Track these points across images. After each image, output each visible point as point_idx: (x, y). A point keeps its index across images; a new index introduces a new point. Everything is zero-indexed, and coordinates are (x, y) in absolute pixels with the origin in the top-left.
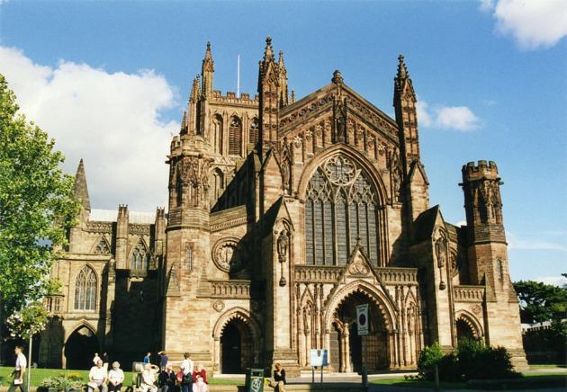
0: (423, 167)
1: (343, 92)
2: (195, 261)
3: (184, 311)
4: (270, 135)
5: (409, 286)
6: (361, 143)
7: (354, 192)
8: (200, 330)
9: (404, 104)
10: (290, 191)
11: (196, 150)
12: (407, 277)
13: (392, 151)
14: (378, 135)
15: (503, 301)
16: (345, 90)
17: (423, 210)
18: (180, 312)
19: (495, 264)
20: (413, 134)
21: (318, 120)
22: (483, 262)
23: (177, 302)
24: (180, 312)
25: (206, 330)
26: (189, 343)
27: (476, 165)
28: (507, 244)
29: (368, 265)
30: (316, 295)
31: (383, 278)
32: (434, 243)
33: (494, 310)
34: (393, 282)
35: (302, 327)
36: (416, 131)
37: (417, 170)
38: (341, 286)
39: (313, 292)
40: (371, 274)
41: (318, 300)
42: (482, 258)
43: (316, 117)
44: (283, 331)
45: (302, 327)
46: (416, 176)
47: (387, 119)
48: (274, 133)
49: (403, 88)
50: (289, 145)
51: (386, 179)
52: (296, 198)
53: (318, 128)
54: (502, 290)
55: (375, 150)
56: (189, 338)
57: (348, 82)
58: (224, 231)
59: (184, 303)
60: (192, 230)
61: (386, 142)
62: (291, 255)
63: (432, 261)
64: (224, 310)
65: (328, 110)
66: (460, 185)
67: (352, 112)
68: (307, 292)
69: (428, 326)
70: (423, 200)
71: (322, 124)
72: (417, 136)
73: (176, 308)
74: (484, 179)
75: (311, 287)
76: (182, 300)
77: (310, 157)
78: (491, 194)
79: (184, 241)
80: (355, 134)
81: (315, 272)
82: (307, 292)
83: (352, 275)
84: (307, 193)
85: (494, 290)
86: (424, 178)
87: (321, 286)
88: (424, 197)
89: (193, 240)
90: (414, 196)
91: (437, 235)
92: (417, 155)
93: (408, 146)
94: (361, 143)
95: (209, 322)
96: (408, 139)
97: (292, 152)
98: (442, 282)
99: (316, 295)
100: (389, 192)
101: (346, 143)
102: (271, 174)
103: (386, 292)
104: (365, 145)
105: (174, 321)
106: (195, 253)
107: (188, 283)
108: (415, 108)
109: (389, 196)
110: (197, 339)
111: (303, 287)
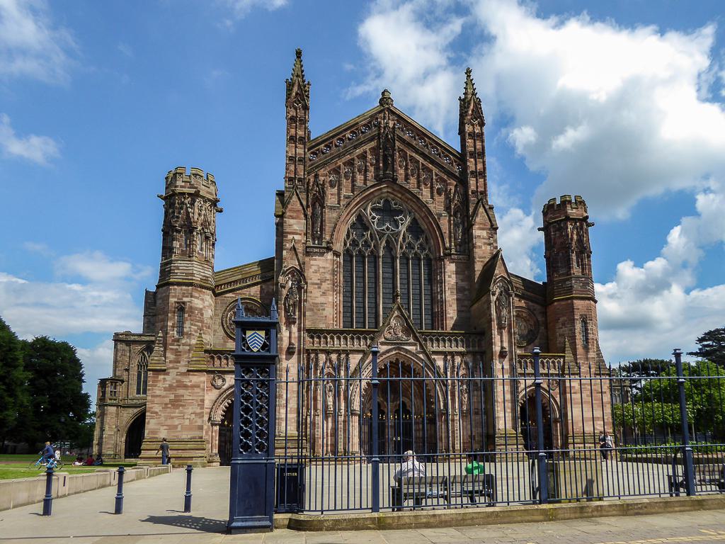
0: (491, 208)
2: (187, 325)
3: (171, 388)
4: (296, 169)
6: (413, 180)
7: (404, 241)
8: (191, 411)
9: (468, 128)
10: (320, 238)
14: (435, 170)
16: (393, 113)
18: (165, 389)
19: (578, 326)
20: (480, 166)
21: (359, 151)
23: (161, 377)
24: (165, 389)
25: (198, 411)
26: (176, 427)
27: (558, 202)
28: (596, 302)
29: (408, 330)
30: (339, 366)
31: (429, 344)
32: (494, 298)
34: (441, 349)
35: (320, 406)
36: (484, 163)
37: (481, 210)
40: (412, 340)
41: (342, 373)
43: (355, 147)
45: (320, 406)
46: (481, 218)
47: (446, 150)
49: (469, 107)
51: (444, 223)
52: (329, 249)
53: (358, 163)
55: (432, 188)
56: (176, 422)
59: (170, 378)
60: (184, 287)
61: (445, 177)
62: (302, 315)
63: (490, 321)
64: (225, 387)
65: (371, 139)
66: (539, 229)
70: (488, 247)
71: (363, 156)
72: (484, 168)
73: (160, 384)
74: (568, 218)
76: (168, 374)
77: (348, 197)
78: (575, 237)
79: (172, 300)
80: (406, 169)
81: (339, 338)
82: (328, 364)
84: (345, 244)
85: (576, 359)
86: (490, 220)
87: (347, 355)
88: (490, 244)
89: (185, 299)
90: (478, 242)
91: (496, 289)
92: (484, 193)
93: (472, 182)
95: (203, 401)
96: (472, 172)
97: (324, 192)
98: (502, 348)
100: (447, 240)
101: (395, 180)
102: (293, 218)
103: (432, 362)
104: (419, 182)
105: (156, 400)
106: (186, 315)
107: (177, 353)
108: (482, 134)
109: (448, 245)
110: (187, 422)
111: (322, 357)
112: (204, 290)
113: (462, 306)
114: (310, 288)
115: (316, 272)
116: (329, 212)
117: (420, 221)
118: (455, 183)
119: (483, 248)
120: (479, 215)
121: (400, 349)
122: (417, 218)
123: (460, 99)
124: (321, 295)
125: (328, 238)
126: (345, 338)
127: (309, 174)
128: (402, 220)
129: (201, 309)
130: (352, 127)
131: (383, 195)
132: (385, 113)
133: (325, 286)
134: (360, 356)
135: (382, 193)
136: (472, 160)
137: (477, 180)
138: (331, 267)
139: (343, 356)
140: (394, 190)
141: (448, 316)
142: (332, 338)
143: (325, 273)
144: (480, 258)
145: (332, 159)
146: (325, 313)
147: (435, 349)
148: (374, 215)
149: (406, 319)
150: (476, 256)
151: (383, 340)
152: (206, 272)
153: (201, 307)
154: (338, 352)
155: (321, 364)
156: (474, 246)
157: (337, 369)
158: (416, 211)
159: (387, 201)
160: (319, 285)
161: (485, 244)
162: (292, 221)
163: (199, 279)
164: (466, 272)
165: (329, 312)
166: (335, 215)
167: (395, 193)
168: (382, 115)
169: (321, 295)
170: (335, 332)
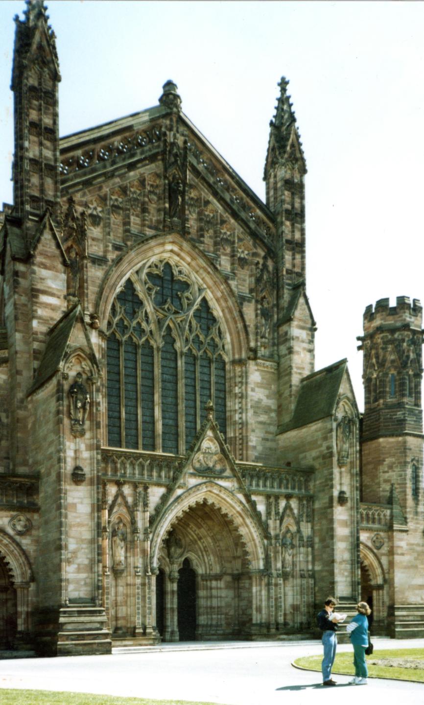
12: (285, 482)
13: (261, 261)
15: (415, 530)
17: (307, 373)
22: (391, 467)
38: (179, 492)
39: (130, 500)
42: (388, 461)
54: (416, 513)
68: (120, 500)
69: (313, 564)
70: (308, 355)
75: (127, 490)
81: (132, 464)
84: (110, 324)
87: (146, 488)
111: (112, 490)
119: (302, 355)
120: (299, 307)
122: (208, 299)
126: (142, 466)
139: (140, 489)
141: (250, 444)
142: (123, 463)
144: (298, 368)
150: (294, 365)
151: (191, 471)
155: (110, 499)
156: (290, 351)
157: (131, 510)
158: (209, 287)
161: (304, 349)
164: (273, 387)
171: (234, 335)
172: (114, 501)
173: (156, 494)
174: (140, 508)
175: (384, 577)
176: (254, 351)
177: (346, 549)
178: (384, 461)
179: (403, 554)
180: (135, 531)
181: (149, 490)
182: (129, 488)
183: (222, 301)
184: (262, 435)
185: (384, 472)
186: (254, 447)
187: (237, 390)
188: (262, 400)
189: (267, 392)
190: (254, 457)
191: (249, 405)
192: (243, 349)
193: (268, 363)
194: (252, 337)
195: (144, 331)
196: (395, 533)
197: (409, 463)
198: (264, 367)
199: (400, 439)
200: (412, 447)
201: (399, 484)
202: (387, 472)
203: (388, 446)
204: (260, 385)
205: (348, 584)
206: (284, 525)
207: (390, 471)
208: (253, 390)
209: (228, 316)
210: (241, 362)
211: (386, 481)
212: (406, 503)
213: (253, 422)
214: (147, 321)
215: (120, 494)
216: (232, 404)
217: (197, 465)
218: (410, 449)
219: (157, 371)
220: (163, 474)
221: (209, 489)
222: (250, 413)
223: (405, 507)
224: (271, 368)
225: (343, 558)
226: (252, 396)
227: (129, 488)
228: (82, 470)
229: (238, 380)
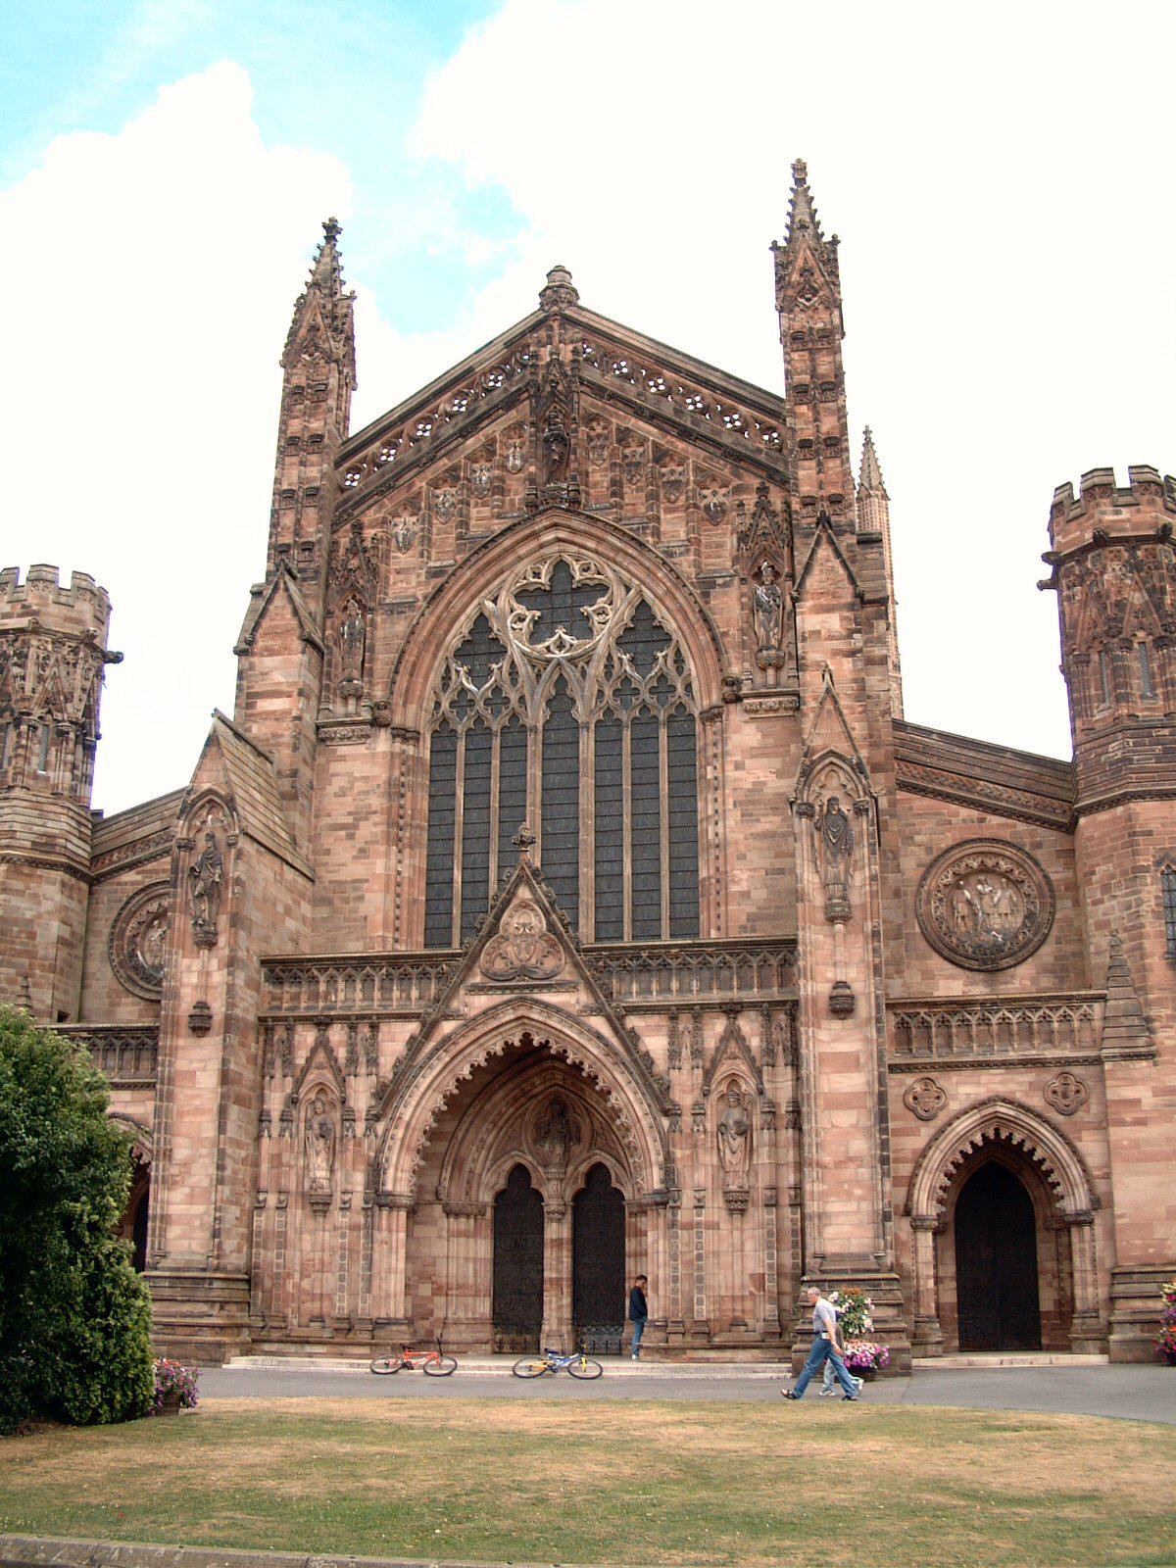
1: (574, 333)
4: (298, 521)
5: (732, 1010)
7: (608, 674)
11: (27, 611)
21: (472, 443)
29: (560, 934)
33: (1143, 1093)
34: (655, 999)
38: (448, 1027)
39: (342, 1053)
40: (567, 974)
43: (464, 433)
44: (191, 1199)
48: (311, 514)
50: (368, 544)
52: (376, 723)
57: (598, 298)
58: (149, 866)
65: (510, 402)
67: (599, 391)
68: (321, 1056)
71: (489, 449)
81: (350, 979)
82: (321, 1056)
83: (496, 982)
87: (374, 1028)
94: (633, 496)
99: (352, 1060)
102: (271, 652)
103: (631, 1039)
111: (307, 1036)
112: (39, 872)
113: (777, 856)
114: (328, 840)
115: (342, 793)
116: (384, 621)
117: (659, 611)
118: (756, 483)
121: (523, 999)
123: (775, 247)
124: (355, 858)
125: (379, 693)
127: (335, 527)
128: (602, 612)
129: (31, 921)
130: (458, 381)
131: (546, 551)
132: (551, 328)
133: (372, 829)
134: (413, 1027)
135: (541, 546)
136: (804, 409)
137: (819, 464)
138: (384, 776)
139: (364, 1030)
140: (574, 531)
141: (734, 888)
143: (367, 793)
145: (398, 476)
146: (364, 908)
147: (635, 1000)
148: (520, 609)
149: (547, 914)
152: (50, 823)
153: (29, 915)
154: (352, 1022)
159: (561, 566)
160: (350, 830)
161: (836, 653)
162: (269, 662)
163: (28, 844)
165: (375, 904)
166: (401, 627)
167: (578, 539)
168: (542, 333)
169: (355, 858)
170: (394, 961)
171: (697, 660)
172: (309, 1060)
173: (395, 1040)
174: (362, 1070)
175: (1091, 1191)
176: (735, 683)
177: (856, 1127)
178: (1093, 873)
179: (1140, 1122)
180: (349, 1117)
181: (384, 1028)
182: (342, 1029)
183: (668, 601)
184: (766, 863)
185: (1095, 903)
186: (746, 895)
187: (710, 773)
188: (764, 783)
189: (777, 763)
190: (743, 919)
191: (730, 801)
192: (714, 684)
193: (771, 701)
194: (732, 654)
195: (507, 700)
196: (1108, 1066)
197: (1145, 869)
198: (767, 711)
199: (1120, 810)
200: (1152, 826)
201: (1126, 930)
202: (1102, 902)
203: (1096, 835)
204: (756, 753)
205: (865, 1219)
206: (724, 1069)
207: (1106, 897)
208: (739, 766)
209: (685, 628)
210: (712, 715)
211: (1102, 925)
212: (1144, 979)
213: (742, 836)
214: (514, 681)
215: (323, 1044)
216: (705, 806)
217: (499, 965)
218: (1150, 833)
219: (534, 772)
220: (415, 994)
221: (521, 1012)
222: (733, 818)
223: (1143, 989)
224: (786, 709)
225: (847, 1152)
226: (736, 780)
227: (342, 1029)
228: (208, 1008)
229: (711, 751)
